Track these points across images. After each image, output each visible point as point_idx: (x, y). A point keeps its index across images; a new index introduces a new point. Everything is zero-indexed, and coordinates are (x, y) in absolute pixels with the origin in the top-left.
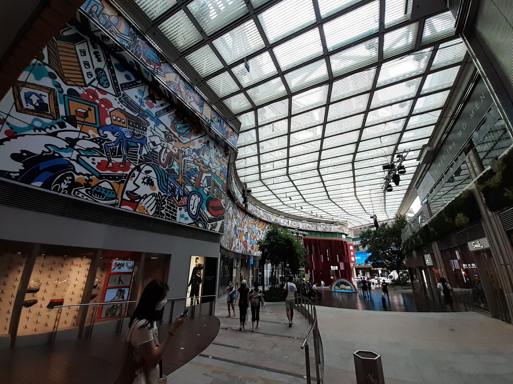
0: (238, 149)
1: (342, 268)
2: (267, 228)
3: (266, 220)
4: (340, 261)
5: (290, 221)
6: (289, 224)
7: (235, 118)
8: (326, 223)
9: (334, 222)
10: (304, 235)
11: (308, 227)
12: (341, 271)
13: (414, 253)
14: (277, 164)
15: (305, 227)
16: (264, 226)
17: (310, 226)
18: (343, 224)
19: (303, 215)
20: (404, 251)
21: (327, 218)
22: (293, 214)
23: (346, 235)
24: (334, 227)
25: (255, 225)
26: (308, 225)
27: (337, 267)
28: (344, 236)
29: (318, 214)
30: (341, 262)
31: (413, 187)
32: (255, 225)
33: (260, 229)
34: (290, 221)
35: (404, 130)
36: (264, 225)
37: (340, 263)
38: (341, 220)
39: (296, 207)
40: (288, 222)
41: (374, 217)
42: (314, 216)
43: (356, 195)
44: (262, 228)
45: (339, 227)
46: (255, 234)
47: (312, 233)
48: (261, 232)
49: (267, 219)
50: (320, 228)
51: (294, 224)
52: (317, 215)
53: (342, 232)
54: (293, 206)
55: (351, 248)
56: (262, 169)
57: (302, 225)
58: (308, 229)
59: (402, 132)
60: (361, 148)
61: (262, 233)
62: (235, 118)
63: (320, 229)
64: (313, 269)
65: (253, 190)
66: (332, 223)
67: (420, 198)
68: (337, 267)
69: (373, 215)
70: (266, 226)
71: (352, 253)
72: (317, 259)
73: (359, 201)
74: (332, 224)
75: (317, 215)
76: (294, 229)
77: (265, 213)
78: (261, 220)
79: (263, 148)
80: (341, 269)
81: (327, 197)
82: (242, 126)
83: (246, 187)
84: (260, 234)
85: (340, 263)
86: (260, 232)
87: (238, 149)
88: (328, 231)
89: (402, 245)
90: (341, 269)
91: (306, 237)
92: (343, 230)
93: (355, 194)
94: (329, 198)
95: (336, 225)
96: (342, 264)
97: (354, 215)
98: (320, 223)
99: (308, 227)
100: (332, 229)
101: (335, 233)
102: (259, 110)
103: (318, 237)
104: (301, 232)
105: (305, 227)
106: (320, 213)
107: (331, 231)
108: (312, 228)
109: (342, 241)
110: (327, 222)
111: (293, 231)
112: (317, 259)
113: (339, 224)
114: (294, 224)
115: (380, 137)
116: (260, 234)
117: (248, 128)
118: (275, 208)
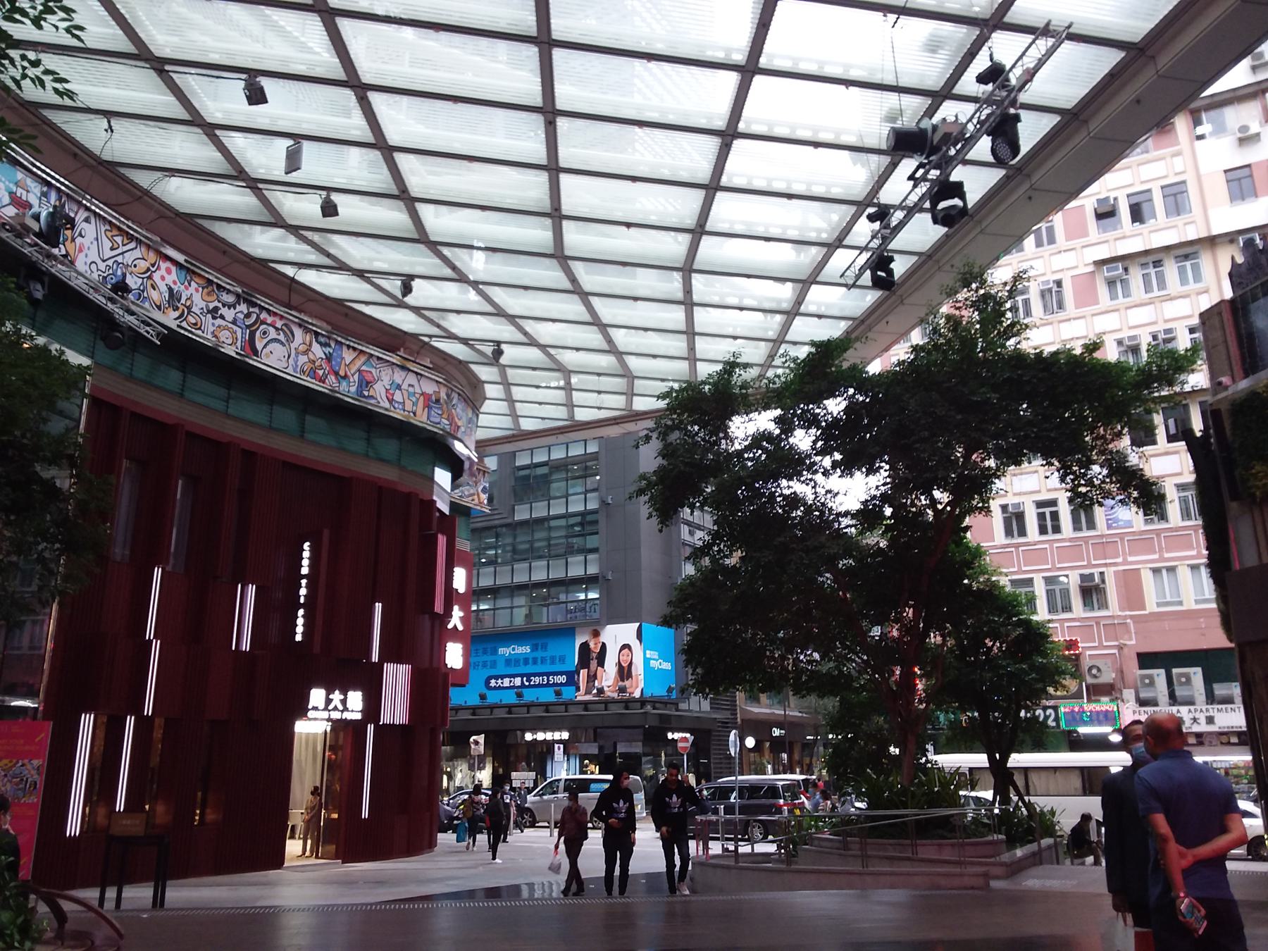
1: (395, 710)
4: (392, 653)
11: (173, 297)
12: (382, 731)
17: (195, 295)
24: (399, 376)
26: (166, 277)
27: (356, 700)
30: (399, 661)
37: (389, 668)
45: (429, 388)
64: (137, 709)
66: (391, 339)
68: (356, 700)
80: (386, 718)
85: (389, 668)
88: (348, 391)
90: (386, 718)
92: (451, 418)
96: (396, 678)
99: (173, 297)
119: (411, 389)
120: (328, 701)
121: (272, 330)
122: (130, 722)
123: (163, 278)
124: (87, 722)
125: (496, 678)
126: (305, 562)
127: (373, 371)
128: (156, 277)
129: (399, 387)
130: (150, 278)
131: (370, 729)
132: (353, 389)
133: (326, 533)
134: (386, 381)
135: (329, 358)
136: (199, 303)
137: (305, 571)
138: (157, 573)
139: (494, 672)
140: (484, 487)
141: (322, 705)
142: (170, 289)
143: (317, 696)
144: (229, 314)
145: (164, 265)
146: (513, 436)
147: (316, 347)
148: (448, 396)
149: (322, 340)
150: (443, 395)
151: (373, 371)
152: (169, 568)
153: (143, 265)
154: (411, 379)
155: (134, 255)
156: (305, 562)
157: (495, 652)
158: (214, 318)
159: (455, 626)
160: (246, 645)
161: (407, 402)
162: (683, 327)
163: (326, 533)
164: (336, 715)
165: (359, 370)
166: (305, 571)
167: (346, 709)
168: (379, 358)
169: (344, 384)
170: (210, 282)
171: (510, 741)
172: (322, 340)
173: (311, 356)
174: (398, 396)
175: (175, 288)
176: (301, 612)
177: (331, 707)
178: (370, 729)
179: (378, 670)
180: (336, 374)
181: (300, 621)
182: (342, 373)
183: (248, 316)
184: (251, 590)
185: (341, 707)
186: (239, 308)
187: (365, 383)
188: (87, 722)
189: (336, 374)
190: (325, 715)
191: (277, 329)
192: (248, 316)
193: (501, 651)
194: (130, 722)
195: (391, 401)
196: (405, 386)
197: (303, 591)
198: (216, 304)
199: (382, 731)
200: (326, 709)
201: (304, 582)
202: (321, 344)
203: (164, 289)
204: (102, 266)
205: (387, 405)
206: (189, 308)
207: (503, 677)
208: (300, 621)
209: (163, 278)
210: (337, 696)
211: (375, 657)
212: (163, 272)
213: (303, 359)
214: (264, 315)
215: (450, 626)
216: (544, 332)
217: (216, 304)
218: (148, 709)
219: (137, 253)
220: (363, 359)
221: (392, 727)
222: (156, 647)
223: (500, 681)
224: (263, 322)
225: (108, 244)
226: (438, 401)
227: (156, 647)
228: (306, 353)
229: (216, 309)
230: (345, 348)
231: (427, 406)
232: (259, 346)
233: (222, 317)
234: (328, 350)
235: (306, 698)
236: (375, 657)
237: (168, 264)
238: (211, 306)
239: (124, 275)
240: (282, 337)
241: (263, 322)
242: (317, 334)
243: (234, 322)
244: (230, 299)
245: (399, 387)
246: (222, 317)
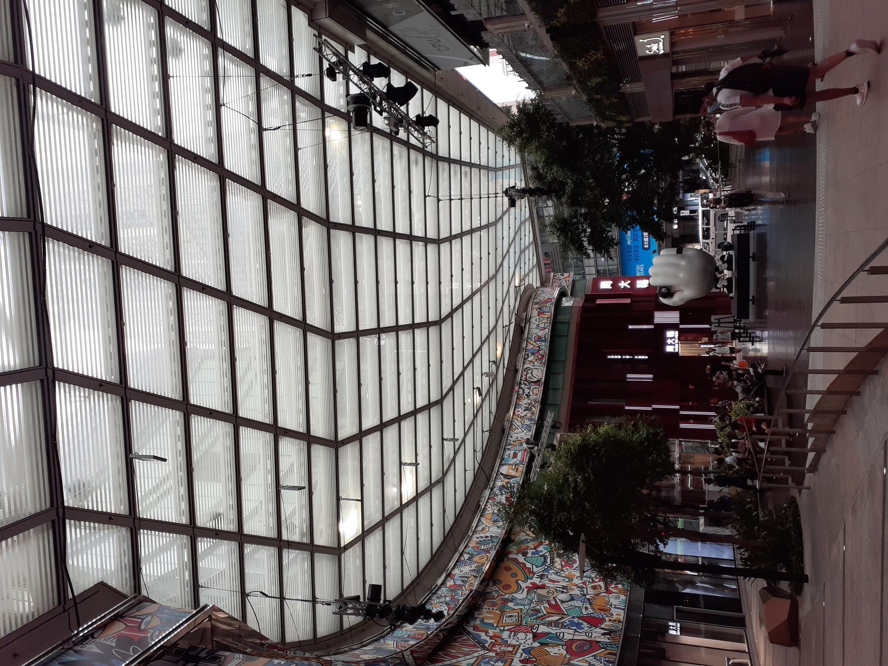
0: (202, 604)
2: (521, 559)
3: (493, 553)
4: (650, 320)
5: (504, 470)
6: (513, 473)
7: (76, 605)
8: (519, 352)
9: (517, 325)
10: (555, 426)
12: (682, 321)
13: (628, 88)
14: (293, 502)
15: (527, 422)
16: (515, 569)
17: (524, 402)
18: (527, 297)
19: (486, 420)
20: (624, 119)
21: (499, 349)
22: (479, 455)
23: (562, 294)
25: (507, 601)
26: (521, 412)
27: (670, 334)
28: (567, 303)
29: (486, 370)
30: (652, 317)
31: (433, 79)
32: (507, 601)
33: (523, 585)
34: (504, 470)
35: (253, 61)
36: (510, 569)
37: (656, 321)
38: (512, 302)
39: (454, 440)
40: (506, 476)
41: (512, 196)
42: (491, 385)
43: (438, 242)
44: (520, 575)
45: (535, 313)
46: (544, 608)
47: (550, 401)
48: (536, 580)
49: (488, 551)
50: (535, 373)
51: (515, 455)
52: (488, 375)
53: (550, 308)
54: (449, 447)
55: (606, 285)
56: (296, 538)
57: (521, 432)
58: (536, 410)
59: (260, 70)
60: (285, 190)
61: (541, 577)
62: (76, 605)
63: (539, 373)
64: (677, 410)
65: (374, 578)
66: (520, 331)
67: (466, 64)
68: (670, 334)
69: (506, 199)
70: (516, 560)
71: (623, 284)
72: (641, 393)
73: (456, 237)
74: (522, 332)
75: (488, 375)
76: (532, 458)
77: (466, 556)
78: (491, 577)
79: (217, 516)
80: (677, 321)
81: (433, 330)
82: (114, 583)
83: (357, 598)
84: (543, 587)
85: (656, 321)
86: (535, 587)
87: (202, 604)
88: (545, 347)
89: (603, 125)
90: (677, 321)
91: (563, 419)
93: (433, 241)
94: (435, 323)
95: (528, 320)
97: (499, 261)
98: (516, 371)
100: (541, 333)
101: (555, 324)
102: (69, 501)
103: (565, 381)
104: (544, 435)
105: (527, 422)
106: (483, 364)
107: (548, 337)
108: (532, 397)
109: (584, 309)
110: (516, 348)
111: (538, 461)
112: (641, 393)
113: (526, 309)
114: (515, 455)
115: (261, 130)
116: (543, 587)
117: (127, 560)
118: (450, 518)
119: (538, 320)
120: (671, 344)
121: (528, 375)
122: (682, 413)
123: (522, 413)
124: (682, 426)
125: (643, 245)
126: (616, 357)
127: (534, 336)
128: (522, 415)
129: (538, 325)
130: (523, 417)
131: (681, 326)
132: (543, 344)
133: (604, 350)
134: (537, 331)
135: (533, 354)
137: (620, 357)
138: (627, 408)
139: (640, 246)
140: (561, 275)
141: (673, 347)
142: (525, 410)
143: (669, 349)
144: (527, 391)
145: (517, 413)
146: (539, 268)
147: (530, 359)
148: (536, 304)
149: (526, 357)
150: (537, 306)
151: (534, 336)
152: (625, 404)
153: (519, 419)
154: (533, 320)
155: (517, 423)
156: (616, 357)
157: (629, 246)
158: (530, 395)
159: (629, 284)
160: (651, 376)
161: (543, 321)
163: (604, 350)
164: (677, 341)
165: (535, 342)
166: (620, 357)
167: (674, 337)
168: (528, 334)
169: (542, 347)
171: (677, 236)
172: (526, 357)
173: (534, 360)
174: (542, 325)
175: (524, 409)
176: (636, 357)
177: (673, 343)
178: (681, 326)
179: (657, 325)
180: (538, 351)
181: (640, 357)
182: (538, 348)
183: (525, 384)
184: (629, 376)
185: (674, 339)
186: (524, 388)
187: (539, 339)
188: (682, 426)
189: (538, 351)
190: (677, 345)
191: (527, 374)
192: (525, 384)
193: (629, 243)
194: (682, 413)
195: (545, 329)
196: (537, 323)
197: (628, 357)
198: (524, 395)
199: (682, 323)
200: (674, 345)
201: (624, 357)
202: (528, 357)
203: (525, 413)
204: (525, 432)
205: (547, 330)
206: (529, 404)
207: (643, 242)
208: (640, 357)
209: (522, 413)
210: (669, 341)
211: (652, 327)
212: (519, 413)
213: (536, 363)
215: (629, 287)
217: (524, 395)
218: (678, 407)
219: (516, 421)
220: (530, 341)
221: (681, 318)
222: (654, 406)
223: (645, 243)
224: (526, 378)
225: (517, 431)
226: (540, 308)
227: (654, 406)
228: (533, 363)
229: (526, 395)
230: (527, 348)
231: (543, 313)
232: (536, 380)
233: (529, 393)
234: (530, 355)
235: (670, 353)
236: (652, 327)
237: (516, 412)
238: (526, 397)
239: (526, 425)
240: (530, 372)
241: (526, 378)
242: (525, 359)
243: (530, 389)
245: (538, 325)
246: (529, 393)
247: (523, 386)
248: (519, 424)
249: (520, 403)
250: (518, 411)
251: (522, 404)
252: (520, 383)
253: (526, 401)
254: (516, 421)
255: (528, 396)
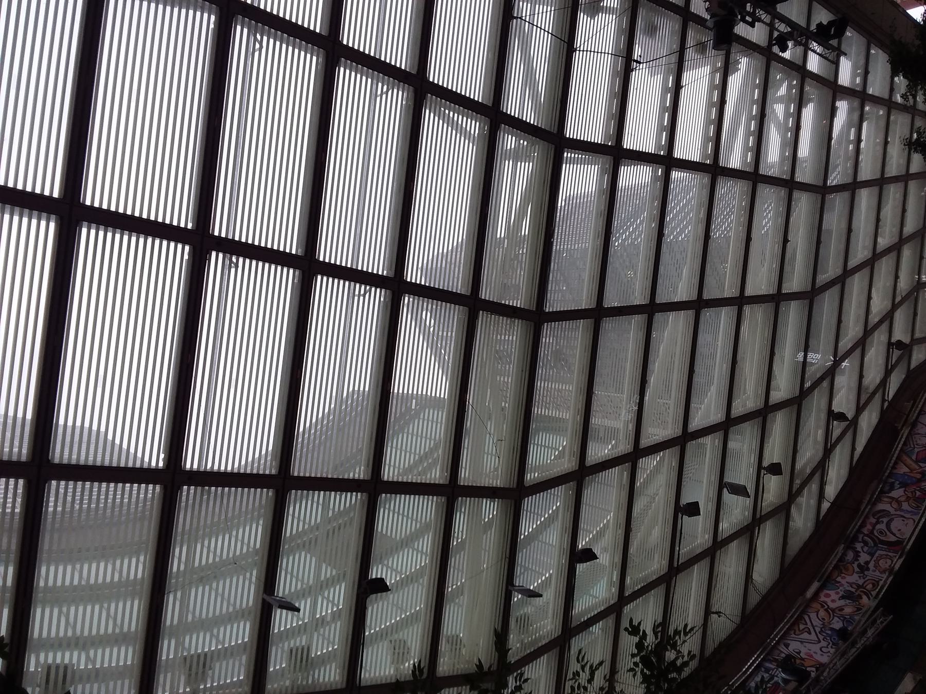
11: (848, 596)
17: (849, 580)
26: (833, 598)
123: (833, 601)
128: (832, 605)
130: (833, 610)
136: (854, 578)
142: (842, 597)
144: (864, 558)
145: (823, 598)
153: (822, 613)
155: (815, 618)
158: (868, 569)
162: (691, 313)
170: (836, 567)
175: (841, 593)
183: (866, 543)
186: (859, 549)
192: (866, 543)
198: (855, 565)
203: (842, 602)
206: (859, 586)
209: (833, 601)
212: (828, 600)
214: (865, 531)
216: (852, 331)
217: (855, 565)
219: (813, 616)
225: (805, 636)
229: (859, 566)
238: (857, 569)
239: (832, 629)
244: (850, 555)
246: (867, 563)
247: (859, 546)
248: (817, 622)
249: (839, 579)
250: (828, 596)
251: (843, 582)
252: (855, 539)
253: (854, 578)
254: (813, 616)
255: (863, 568)
